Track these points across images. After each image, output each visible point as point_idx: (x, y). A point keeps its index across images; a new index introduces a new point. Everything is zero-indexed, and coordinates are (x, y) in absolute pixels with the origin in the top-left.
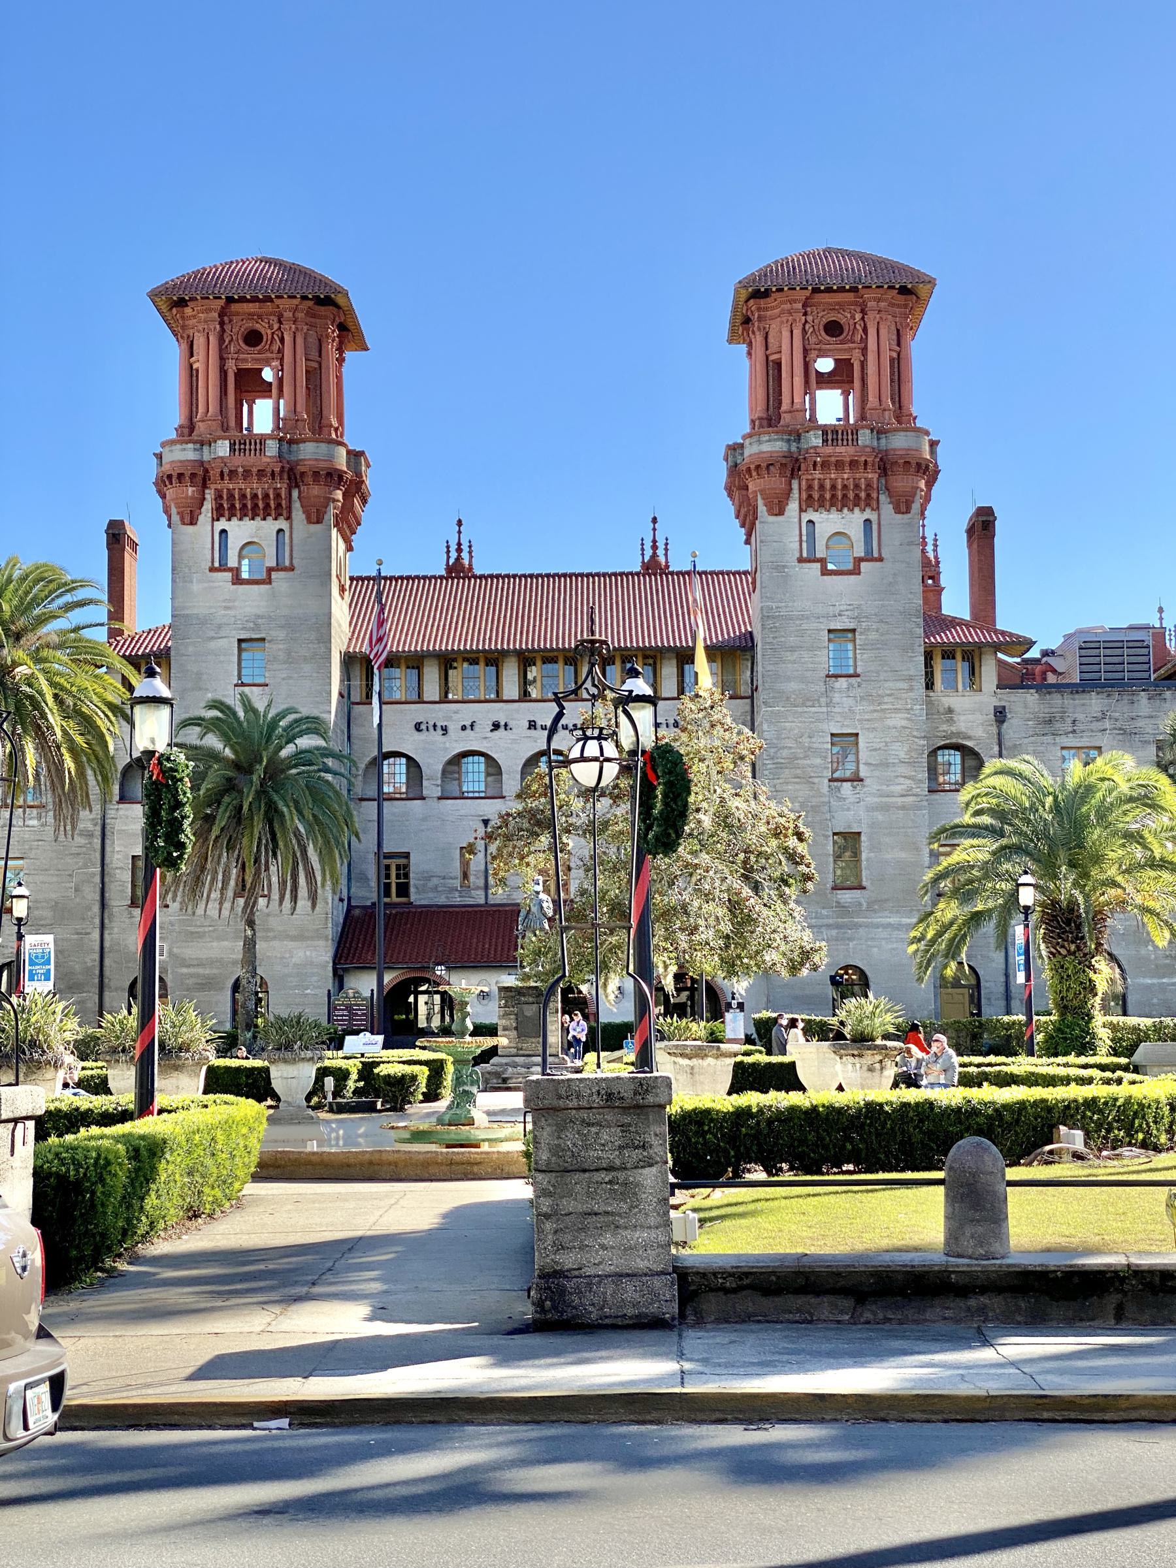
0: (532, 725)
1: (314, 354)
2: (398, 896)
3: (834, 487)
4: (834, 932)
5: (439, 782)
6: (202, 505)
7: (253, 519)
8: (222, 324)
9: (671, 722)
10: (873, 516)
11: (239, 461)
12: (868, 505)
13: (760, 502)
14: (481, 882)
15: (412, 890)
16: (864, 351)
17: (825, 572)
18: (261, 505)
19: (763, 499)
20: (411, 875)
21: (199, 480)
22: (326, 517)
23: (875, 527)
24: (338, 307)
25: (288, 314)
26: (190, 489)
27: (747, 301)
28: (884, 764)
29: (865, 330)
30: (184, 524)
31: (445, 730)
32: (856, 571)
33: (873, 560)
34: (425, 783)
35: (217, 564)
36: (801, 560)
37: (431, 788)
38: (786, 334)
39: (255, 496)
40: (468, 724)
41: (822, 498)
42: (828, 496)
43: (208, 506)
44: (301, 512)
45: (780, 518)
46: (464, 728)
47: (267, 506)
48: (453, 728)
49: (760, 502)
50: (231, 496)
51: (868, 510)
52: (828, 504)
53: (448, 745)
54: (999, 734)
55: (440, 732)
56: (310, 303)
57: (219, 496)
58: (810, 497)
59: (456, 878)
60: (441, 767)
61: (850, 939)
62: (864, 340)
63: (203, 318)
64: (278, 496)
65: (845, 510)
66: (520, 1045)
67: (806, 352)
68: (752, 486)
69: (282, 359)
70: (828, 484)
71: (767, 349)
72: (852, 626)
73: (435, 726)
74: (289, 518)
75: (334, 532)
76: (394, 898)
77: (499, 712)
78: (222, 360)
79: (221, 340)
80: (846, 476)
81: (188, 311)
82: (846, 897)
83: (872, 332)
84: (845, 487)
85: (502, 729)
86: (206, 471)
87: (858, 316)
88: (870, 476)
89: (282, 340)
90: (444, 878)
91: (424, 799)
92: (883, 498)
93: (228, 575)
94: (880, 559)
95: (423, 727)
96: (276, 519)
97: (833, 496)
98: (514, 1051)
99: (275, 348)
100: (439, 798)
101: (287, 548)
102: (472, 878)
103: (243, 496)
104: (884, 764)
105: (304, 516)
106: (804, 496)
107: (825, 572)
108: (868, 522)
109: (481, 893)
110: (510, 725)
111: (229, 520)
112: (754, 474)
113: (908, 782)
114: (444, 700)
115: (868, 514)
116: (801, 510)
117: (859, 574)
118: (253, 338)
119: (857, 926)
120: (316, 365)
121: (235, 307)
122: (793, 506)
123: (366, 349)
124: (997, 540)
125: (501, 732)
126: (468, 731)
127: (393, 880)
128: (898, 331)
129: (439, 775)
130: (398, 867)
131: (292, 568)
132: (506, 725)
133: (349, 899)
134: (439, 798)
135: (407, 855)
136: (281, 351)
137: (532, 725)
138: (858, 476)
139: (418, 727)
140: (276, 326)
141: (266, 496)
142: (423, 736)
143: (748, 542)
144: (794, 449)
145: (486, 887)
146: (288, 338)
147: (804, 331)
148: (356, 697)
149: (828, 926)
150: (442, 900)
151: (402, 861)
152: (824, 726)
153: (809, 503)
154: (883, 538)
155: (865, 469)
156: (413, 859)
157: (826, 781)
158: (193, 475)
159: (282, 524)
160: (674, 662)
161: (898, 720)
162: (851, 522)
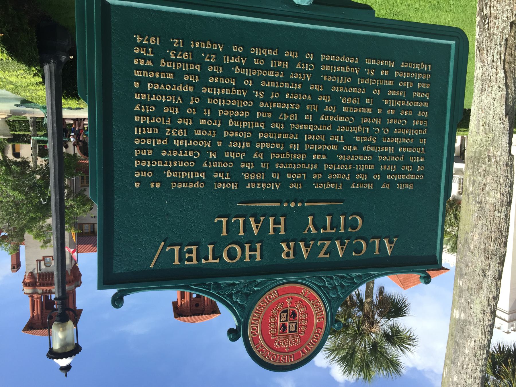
19: (69, 275)
23: (39, 269)
32: (44, 258)
42: (51, 276)
51: (40, 273)
68: (72, 277)
88: (39, 282)
112: (71, 281)
154: (36, 266)
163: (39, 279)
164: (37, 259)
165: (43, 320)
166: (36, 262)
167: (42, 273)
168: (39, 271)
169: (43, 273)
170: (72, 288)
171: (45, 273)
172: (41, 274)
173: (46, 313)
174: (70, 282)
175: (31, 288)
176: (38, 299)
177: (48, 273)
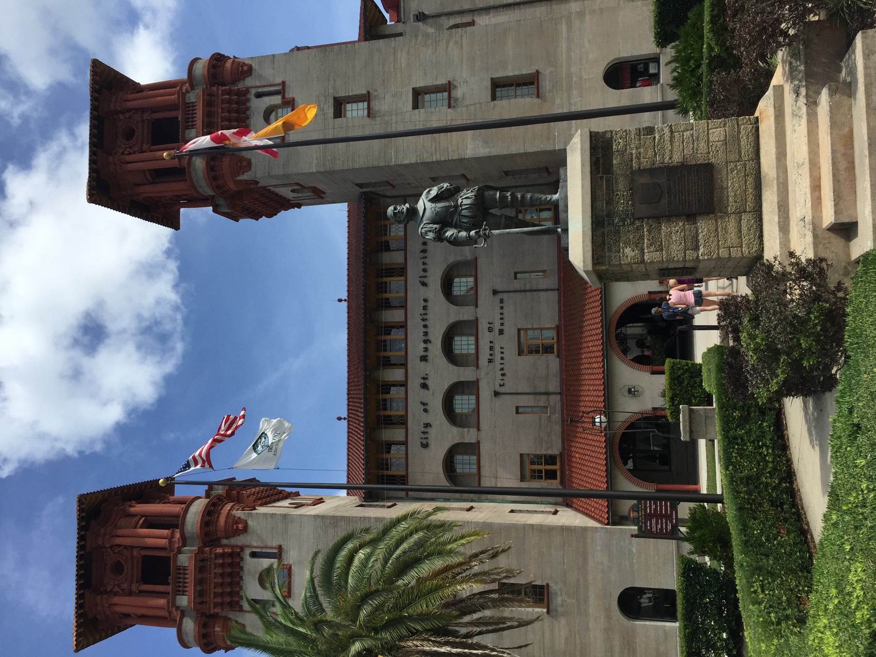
0: (424, 359)
2: (555, 464)
4: (575, 92)
5: (466, 430)
7: (241, 578)
9: (423, 255)
10: (253, 91)
11: (191, 587)
12: (245, 95)
13: (241, 178)
14: (543, 398)
15: (550, 452)
16: (143, 110)
18: (229, 570)
19: (239, 175)
20: (538, 452)
22: (242, 517)
23: (260, 90)
26: (217, 629)
29: (129, 110)
31: (427, 425)
34: (467, 441)
37: (470, 436)
38: (130, 167)
39: (222, 575)
40: (422, 407)
44: (238, 538)
45: (253, 161)
46: (426, 411)
47: (231, 565)
49: (241, 178)
50: (222, 595)
51: (248, 96)
53: (438, 422)
54: (433, 17)
55: (429, 429)
59: (540, 418)
60: (455, 430)
61: (581, 78)
62: (136, 110)
64: (222, 555)
65: (248, 113)
67: (142, 152)
69: (132, 547)
71: (144, 184)
72: (331, 101)
73: (424, 433)
74: (242, 548)
75: (261, 510)
76: (557, 467)
77: (414, 383)
78: (131, 594)
79: (116, 594)
80: (220, 111)
83: (130, 104)
84: (229, 111)
85: (427, 382)
87: (121, 116)
88: (220, 92)
89: (119, 546)
90: (540, 427)
91: (479, 442)
92: (241, 86)
94: (284, 83)
95: (424, 442)
96: (242, 559)
100: (479, 429)
101: (264, 551)
102: (542, 404)
103: (222, 584)
105: (241, 535)
109: (552, 397)
113: (451, 44)
117: (294, 99)
118: (118, 568)
119: (569, 76)
125: (429, 383)
126: (428, 408)
127: (542, 467)
128: (138, 92)
129: (460, 429)
130: (532, 463)
131: (280, 548)
132: (424, 378)
134: (479, 429)
135: (521, 455)
136: (126, 547)
138: (220, 101)
139: (425, 446)
140: (109, 550)
141: (222, 565)
142: (432, 442)
143: (299, 206)
145: (547, 394)
146: (118, 541)
147: (130, 154)
149: (569, 97)
150: (558, 429)
151: (527, 462)
155: (214, 95)
156: (525, 451)
157: (450, 110)
158: (205, 625)
159: (248, 552)
161: (402, 58)
163: (230, 93)
164: (287, 83)
165: (122, 112)
166: (279, 80)
167: (248, 100)
168: (253, 91)
169: (248, 105)
170: (201, 187)
171: (248, 109)
173: (143, 121)
174: (215, 178)
175: (206, 73)
176: (176, 96)
177: (248, 118)
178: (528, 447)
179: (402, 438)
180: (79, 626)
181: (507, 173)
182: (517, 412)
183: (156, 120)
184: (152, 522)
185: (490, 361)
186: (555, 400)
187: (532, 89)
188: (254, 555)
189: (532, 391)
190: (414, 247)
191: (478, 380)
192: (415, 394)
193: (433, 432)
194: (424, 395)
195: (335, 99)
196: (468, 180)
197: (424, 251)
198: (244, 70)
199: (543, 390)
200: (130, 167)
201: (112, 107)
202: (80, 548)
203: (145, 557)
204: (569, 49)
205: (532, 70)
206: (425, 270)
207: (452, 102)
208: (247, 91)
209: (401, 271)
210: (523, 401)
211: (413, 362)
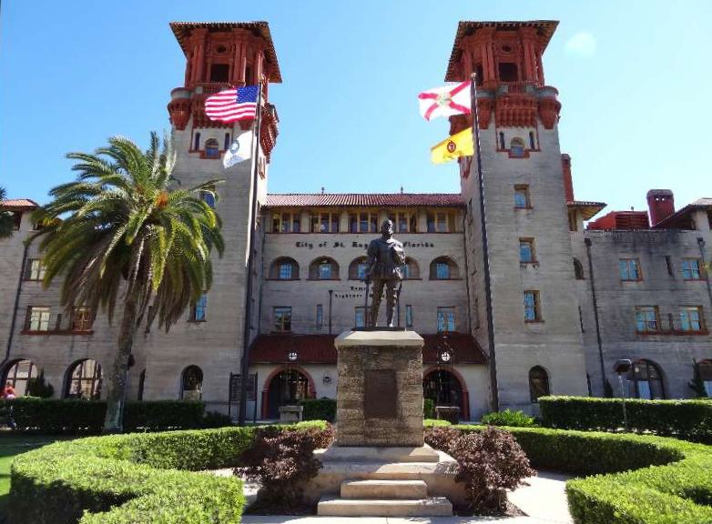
0: (355, 244)
1: (252, 58)
3: (514, 115)
5: (308, 271)
6: (187, 121)
8: (206, 42)
14: (327, 323)
15: (292, 326)
17: (510, 157)
21: (187, 109)
24: (264, 39)
25: (238, 37)
26: (182, 112)
27: (462, 38)
28: (548, 255)
30: (177, 129)
31: (311, 246)
32: (526, 154)
33: (536, 151)
35: (193, 148)
36: (498, 150)
37: (304, 274)
38: (484, 51)
41: (508, 120)
43: (191, 122)
45: (485, 131)
46: (320, 245)
48: (316, 245)
52: (511, 123)
56: (249, 32)
57: (195, 116)
58: (502, 120)
62: (523, 52)
63: (199, 40)
66: (368, 430)
67: (494, 57)
70: (511, 112)
77: (338, 238)
78: (205, 58)
79: (205, 48)
81: (191, 38)
82: (533, 327)
84: (520, 115)
86: (191, 104)
92: (539, 122)
93: (198, 154)
94: (539, 150)
96: (225, 128)
97: (514, 120)
98: (360, 438)
99: (232, 53)
100: (308, 280)
104: (548, 255)
106: (499, 118)
107: (510, 157)
108: (531, 134)
110: (344, 244)
111: (201, 128)
114: (312, 231)
115: (532, 129)
116: (497, 127)
118: (221, 50)
120: (251, 63)
121: (213, 34)
122: (492, 126)
123: (280, 81)
124: (572, 168)
125: (339, 247)
132: (342, 245)
133: (259, 331)
137: (355, 244)
139: (298, 244)
144: (492, 96)
145: (330, 325)
148: (267, 229)
152: (515, 233)
153: (502, 122)
158: (184, 105)
160: (425, 216)
162: (523, 133)
166: (541, 148)
167: (528, 127)
169: (526, 128)
171: (522, 127)
172: (529, 124)
177: (517, 126)
178: (296, 311)
179: (303, 230)
180: (186, 26)
181: (476, 300)
182: (318, 305)
183: (516, 69)
184: (251, 72)
185: (352, 288)
186: (325, 330)
187: (532, 317)
188: (227, 135)
189: (333, 314)
190: (431, 238)
191: (339, 280)
192: (331, 239)
193: (306, 249)
194: (331, 244)
195: (527, 186)
196: (473, 274)
197: (427, 246)
198: (551, 123)
199: (332, 322)
200: (484, 51)
201: (525, 36)
202: (234, 25)
203: (227, 66)
204: (557, 343)
205: (544, 318)
206: (414, 245)
207: (524, 265)
208: (535, 126)
209: (414, 231)
210: (325, 308)
211: (353, 237)
